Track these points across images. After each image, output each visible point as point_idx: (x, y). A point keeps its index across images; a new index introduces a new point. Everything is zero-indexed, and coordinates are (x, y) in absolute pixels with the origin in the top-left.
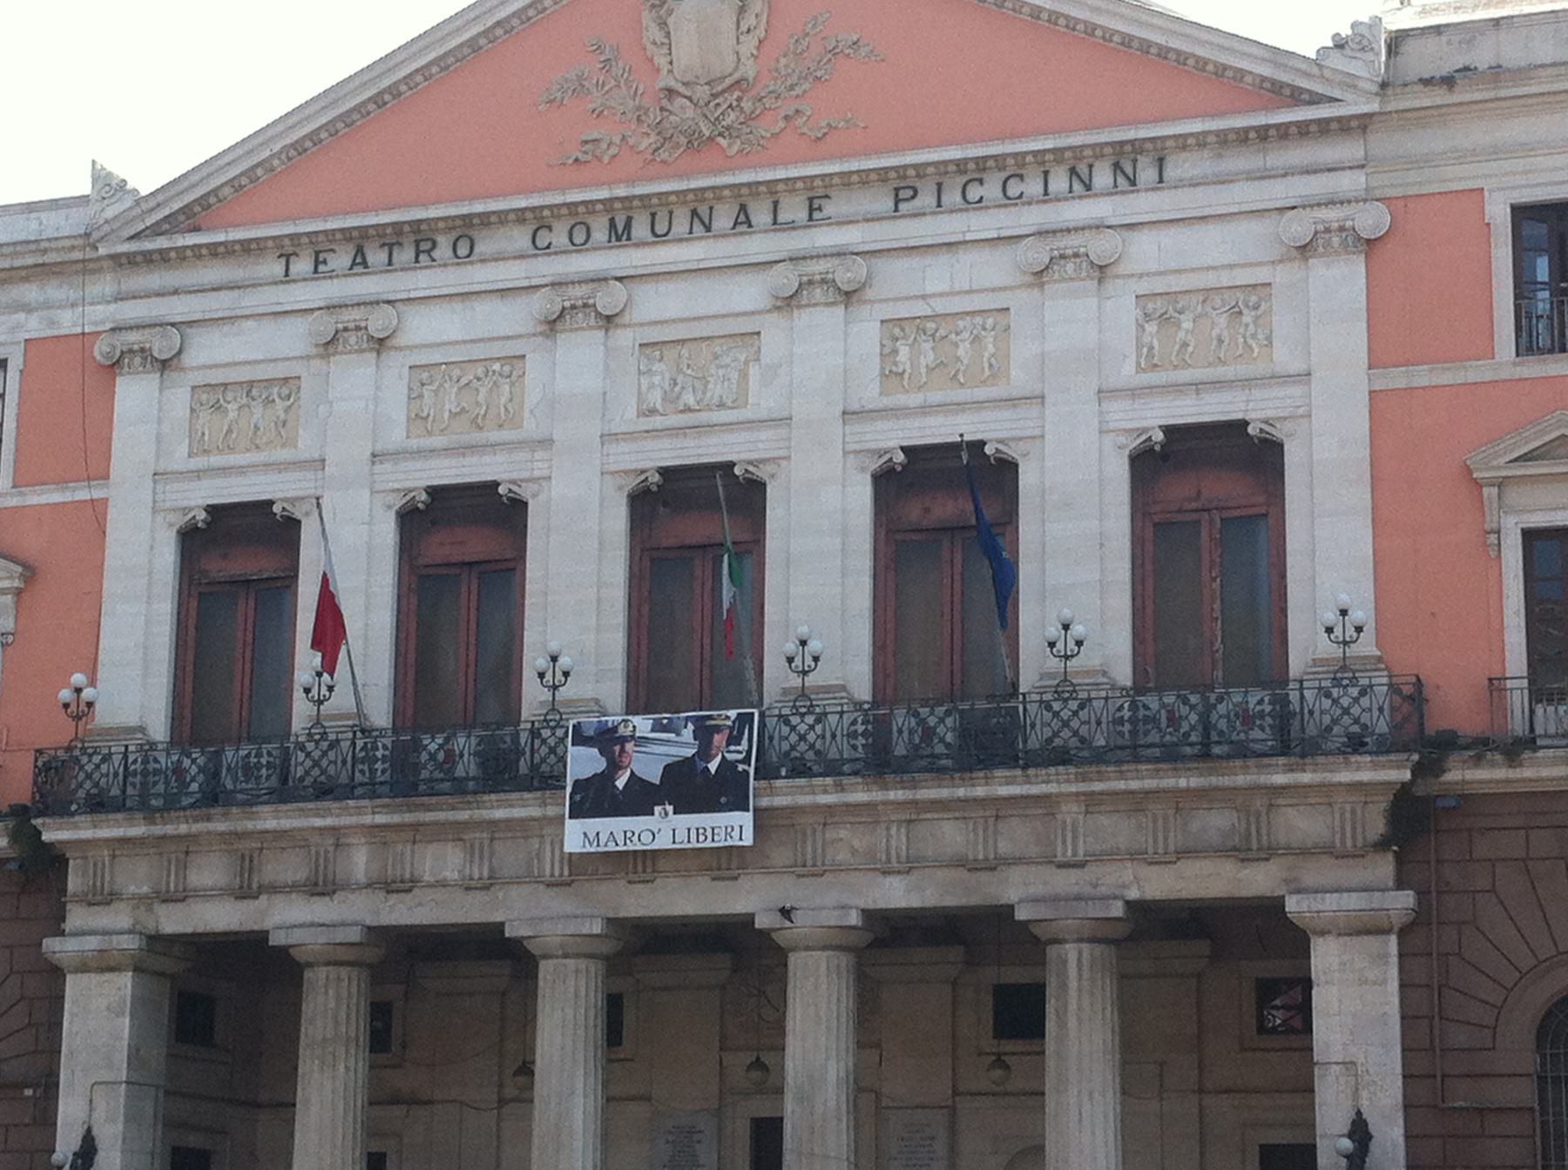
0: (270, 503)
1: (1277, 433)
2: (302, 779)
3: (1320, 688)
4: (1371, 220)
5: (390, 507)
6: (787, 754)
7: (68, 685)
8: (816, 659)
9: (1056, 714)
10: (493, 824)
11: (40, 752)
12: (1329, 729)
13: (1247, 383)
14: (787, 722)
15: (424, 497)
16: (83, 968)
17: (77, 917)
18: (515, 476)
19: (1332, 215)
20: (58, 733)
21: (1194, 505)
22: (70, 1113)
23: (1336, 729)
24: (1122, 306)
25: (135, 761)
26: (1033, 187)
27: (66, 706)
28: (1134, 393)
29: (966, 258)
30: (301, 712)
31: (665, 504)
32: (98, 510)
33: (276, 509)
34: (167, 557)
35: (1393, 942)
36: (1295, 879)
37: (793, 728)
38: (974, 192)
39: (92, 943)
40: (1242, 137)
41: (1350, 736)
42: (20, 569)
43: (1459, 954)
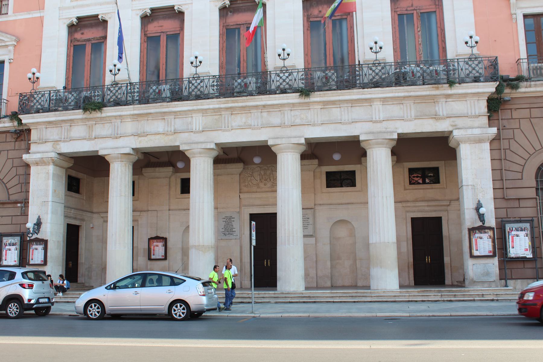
0: (97, 15)
2: (109, 100)
3: (465, 62)
5: (138, 15)
6: (279, 86)
7: (30, 72)
8: (288, 55)
9: (373, 71)
10: (175, 112)
11: (21, 95)
12: (468, 75)
14: (279, 76)
15: (149, 11)
16: (37, 164)
17: (33, 148)
18: (179, 3)
20: (27, 88)
21: (413, 8)
22: (34, 212)
23: (471, 75)
25: (53, 96)
27: (30, 79)
30: (109, 79)
31: (231, 12)
32: (41, 19)
33: (100, 17)
34: (64, 33)
35: (487, 146)
36: (456, 126)
37: (281, 78)
39: (39, 156)
41: (475, 77)
42: (14, 38)
43: (509, 149)
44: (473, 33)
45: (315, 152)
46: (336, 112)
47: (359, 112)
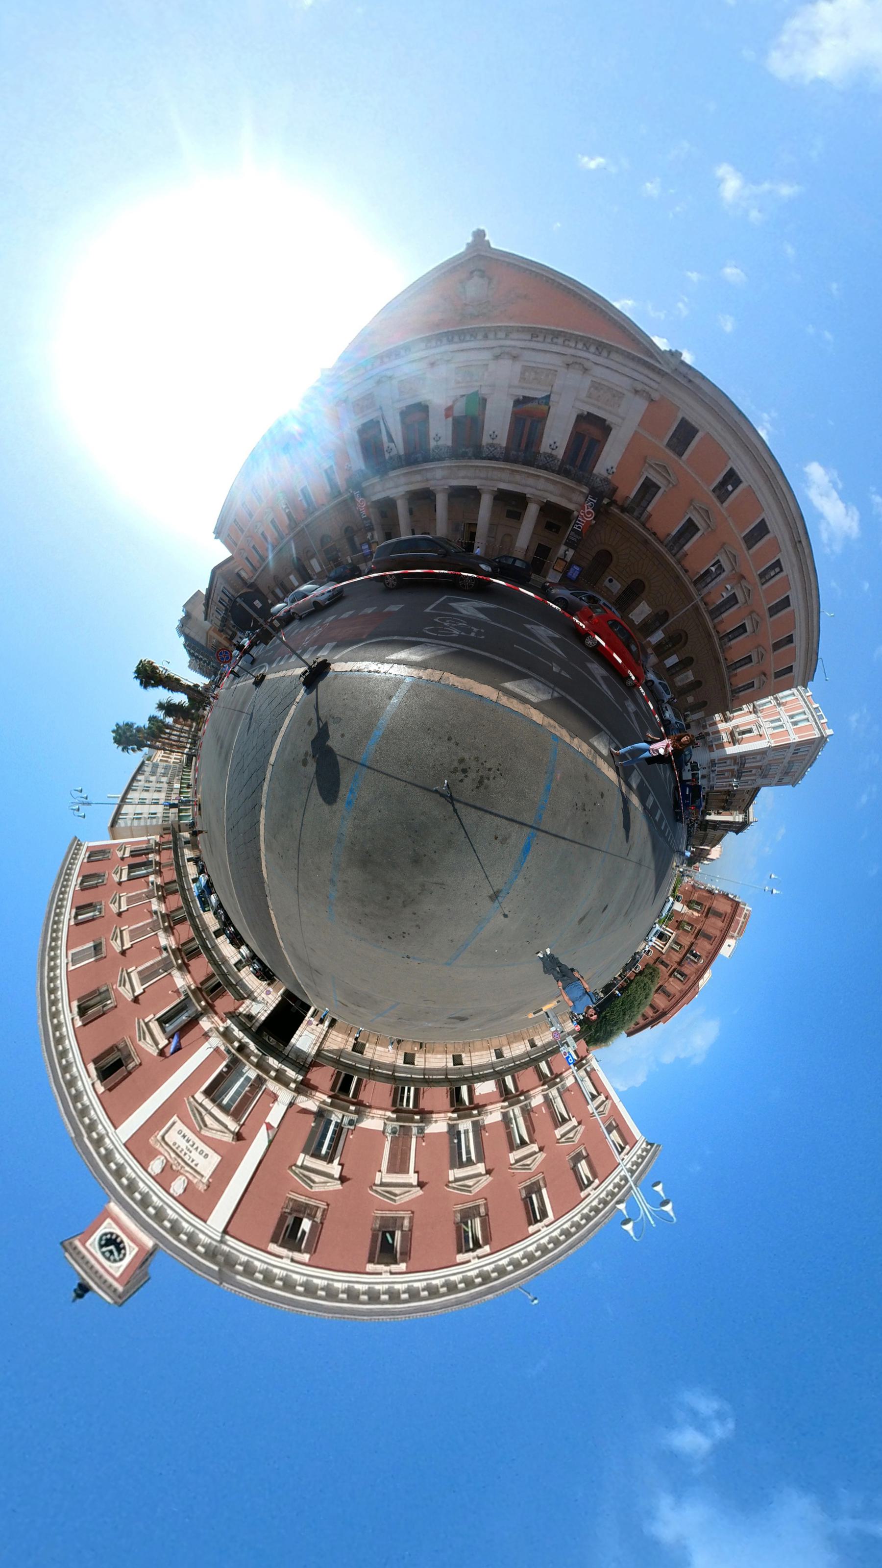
1: (612, 426)
4: (655, 396)
13: (610, 413)
19: (647, 389)
24: (587, 382)
26: (572, 344)
28: (584, 402)
29: (548, 355)
38: (555, 340)
40: (634, 358)
44: (615, 466)
45: (501, 497)
46: (518, 478)
47: (531, 481)
